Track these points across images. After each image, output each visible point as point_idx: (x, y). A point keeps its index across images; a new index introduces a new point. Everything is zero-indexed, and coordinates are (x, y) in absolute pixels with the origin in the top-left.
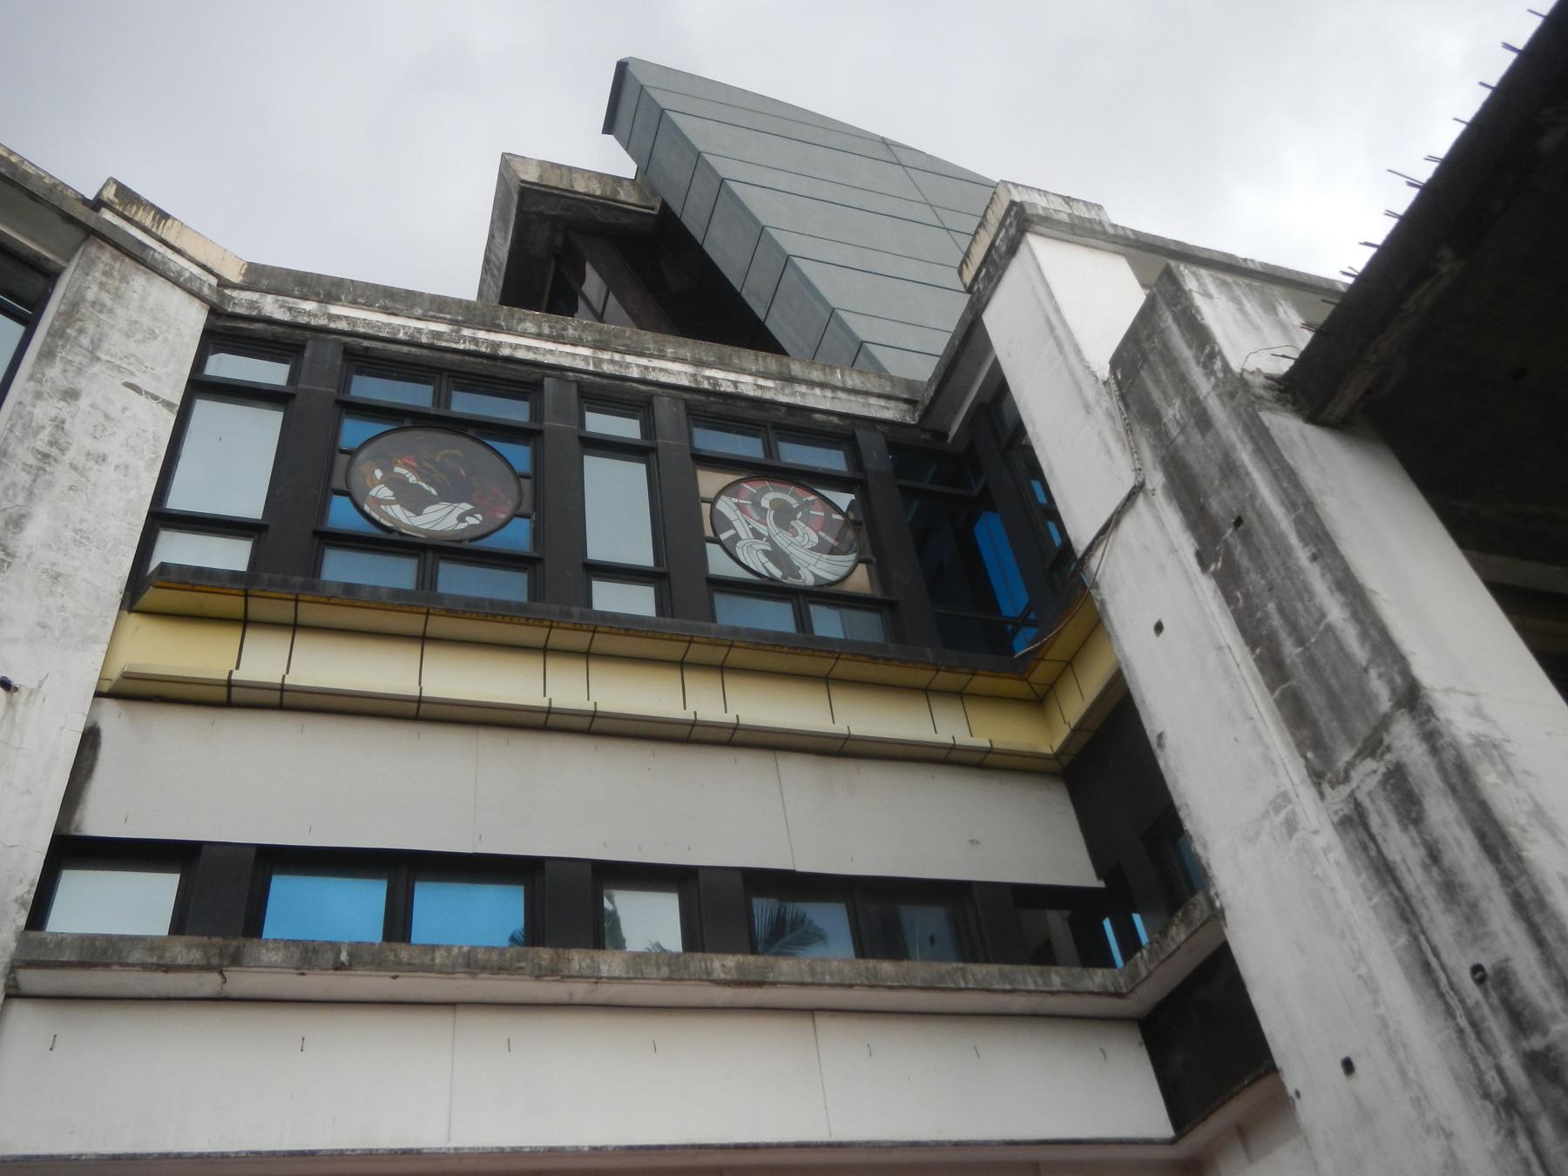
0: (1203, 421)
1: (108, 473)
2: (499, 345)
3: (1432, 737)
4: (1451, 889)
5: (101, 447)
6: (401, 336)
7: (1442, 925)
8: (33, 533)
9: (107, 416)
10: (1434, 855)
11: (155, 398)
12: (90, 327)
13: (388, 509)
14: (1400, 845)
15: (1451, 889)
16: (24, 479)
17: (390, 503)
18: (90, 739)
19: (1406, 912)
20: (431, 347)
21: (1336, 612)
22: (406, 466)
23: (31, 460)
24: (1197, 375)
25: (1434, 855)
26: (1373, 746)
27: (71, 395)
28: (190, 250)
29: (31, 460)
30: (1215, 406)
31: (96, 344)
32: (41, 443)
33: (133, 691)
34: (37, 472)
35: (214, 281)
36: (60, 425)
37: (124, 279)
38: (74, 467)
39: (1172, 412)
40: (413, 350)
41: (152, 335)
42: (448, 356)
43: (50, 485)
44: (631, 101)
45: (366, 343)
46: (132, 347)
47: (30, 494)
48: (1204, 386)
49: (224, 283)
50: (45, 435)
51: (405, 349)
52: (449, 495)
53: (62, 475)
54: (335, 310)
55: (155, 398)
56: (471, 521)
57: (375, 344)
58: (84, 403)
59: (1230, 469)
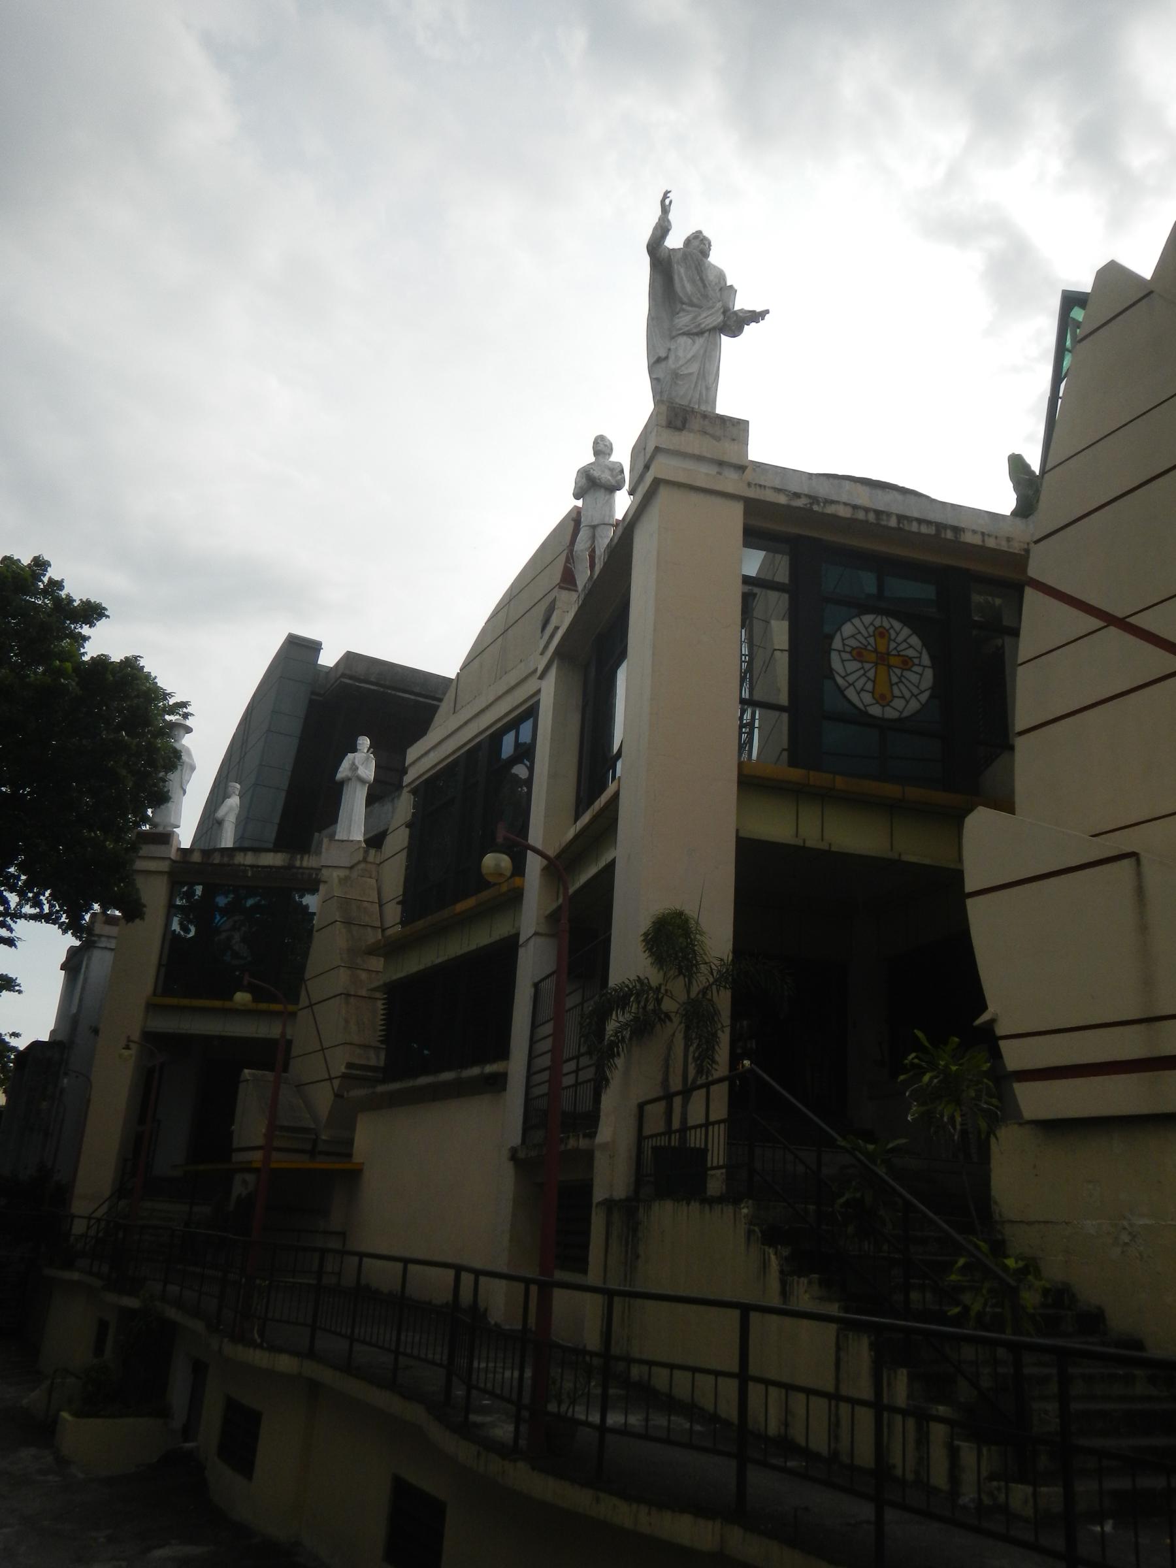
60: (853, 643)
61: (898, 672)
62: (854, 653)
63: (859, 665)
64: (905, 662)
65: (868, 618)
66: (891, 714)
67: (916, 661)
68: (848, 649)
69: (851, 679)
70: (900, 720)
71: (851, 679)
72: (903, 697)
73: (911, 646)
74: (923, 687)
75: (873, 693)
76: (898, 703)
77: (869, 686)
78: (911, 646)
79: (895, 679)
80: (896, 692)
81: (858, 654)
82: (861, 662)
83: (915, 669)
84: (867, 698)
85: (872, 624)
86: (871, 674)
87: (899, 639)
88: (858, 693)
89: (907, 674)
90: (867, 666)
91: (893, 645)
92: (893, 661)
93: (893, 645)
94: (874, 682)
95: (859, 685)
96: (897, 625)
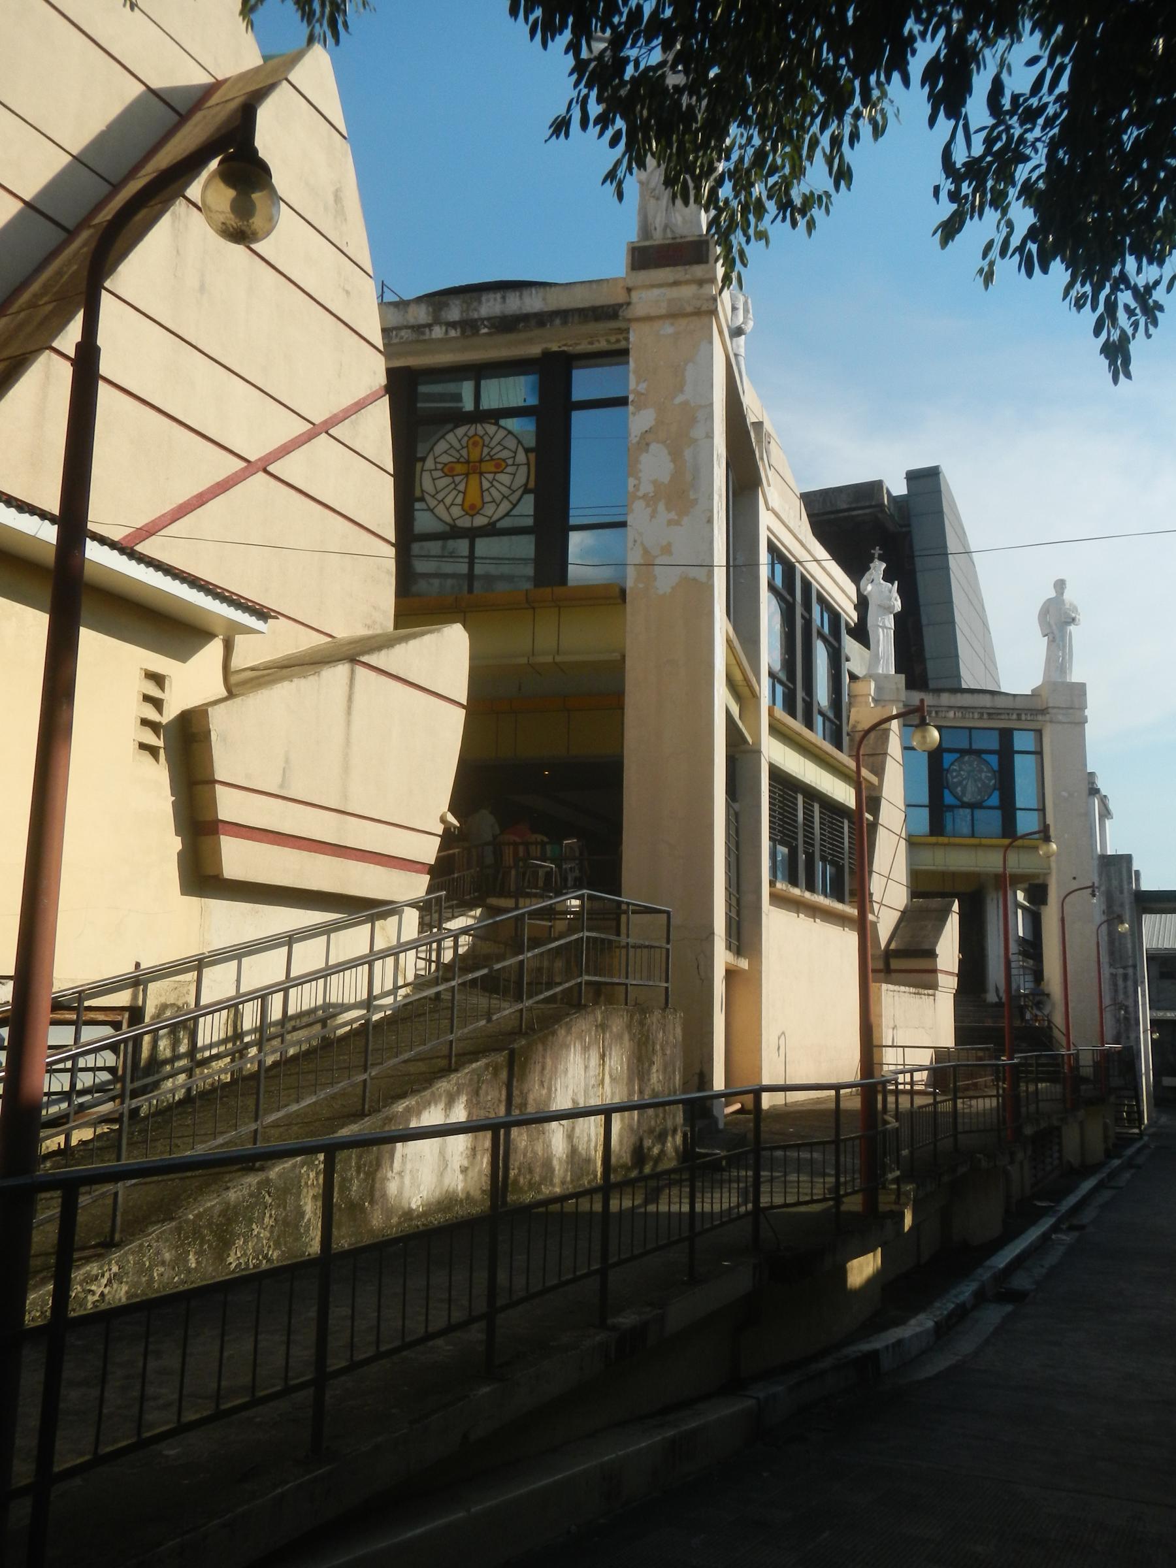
0: (1122, 892)
3: (1135, 974)
4: (1125, 993)
7: (1121, 997)
10: (1125, 988)
14: (1120, 982)
15: (1125, 993)
19: (1116, 991)
21: (1129, 946)
24: (1125, 883)
25: (1125, 988)
26: (1125, 968)
30: (1126, 891)
39: (1115, 883)
44: (926, 481)
48: (1126, 887)
59: (1122, 905)
60: (445, 459)
61: (490, 477)
62: (446, 470)
63: (448, 480)
64: (497, 466)
65: (461, 431)
66: (480, 521)
67: (510, 462)
68: (439, 466)
69: (440, 496)
70: (489, 524)
71: (440, 496)
72: (494, 501)
73: (505, 448)
74: (514, 487)
75: (462, 505)
76: (489, 510)
77: (459, 500)
78: (505, 448)
79: (486, 485)
80: (487, 499)
81: (448, 471)
82: (453, 476)
83: (509, 469)
84: (456, 511)
85: (465, 435)
86: (461, 487)
87: (493, 444)
88: (448, 509)
89: (500, 477)
90: (457, 479)
91: (486, 450)
92: (485, 467)
93: (486, 450)
94: (464, 493)
95: (448, 501)
96: (491, 429)
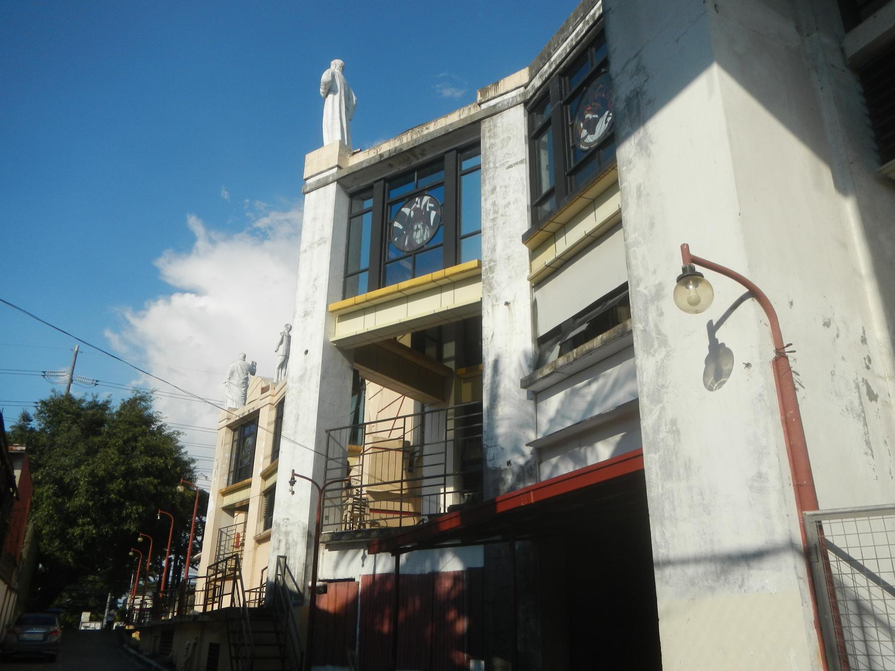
1: (512, 207)
2: (594, 14)
5: (507, 200)
6: (568, 50)
8: (499, 248)
9: (506, 187)
11: (516, 164)
12: (491, 158)
13: (586, 141)
16: (491, 232)
17: (586, 136)
18: (534, 305)
20: (578, 43)
22: (589, 112)
23: (491, 224)
27: (494, 189)
28: (509, 89)
29: (491, 224)
31: (494, 163)
32: (492, 217)
33: (539, 281)
34: (493, 228)
35: (522, 89)
36: (494, 204)
37: (495, 126)
38: (502, 215)
40: (575, 51)
41: (509, 138)
42: (584, 41)
43: (498, 228)
45: (562, 66)
46: (505, 151)
47: (494, 236)
49: (526, 86)
50: (491, 213)
51: (572, 55)
52: (601, 115)
53: (500, 221)
54: (552, 59)
55: (516, 164)
56: (609, 119)
57: (565, 62)
58: (498, 189)
